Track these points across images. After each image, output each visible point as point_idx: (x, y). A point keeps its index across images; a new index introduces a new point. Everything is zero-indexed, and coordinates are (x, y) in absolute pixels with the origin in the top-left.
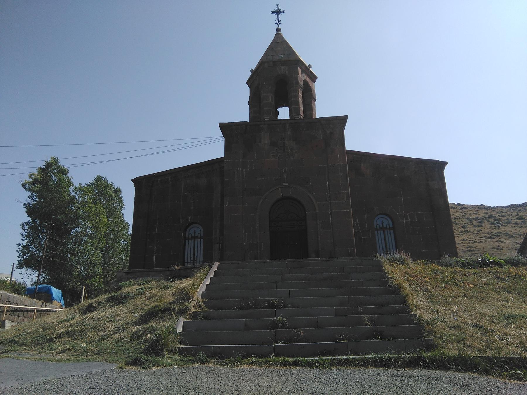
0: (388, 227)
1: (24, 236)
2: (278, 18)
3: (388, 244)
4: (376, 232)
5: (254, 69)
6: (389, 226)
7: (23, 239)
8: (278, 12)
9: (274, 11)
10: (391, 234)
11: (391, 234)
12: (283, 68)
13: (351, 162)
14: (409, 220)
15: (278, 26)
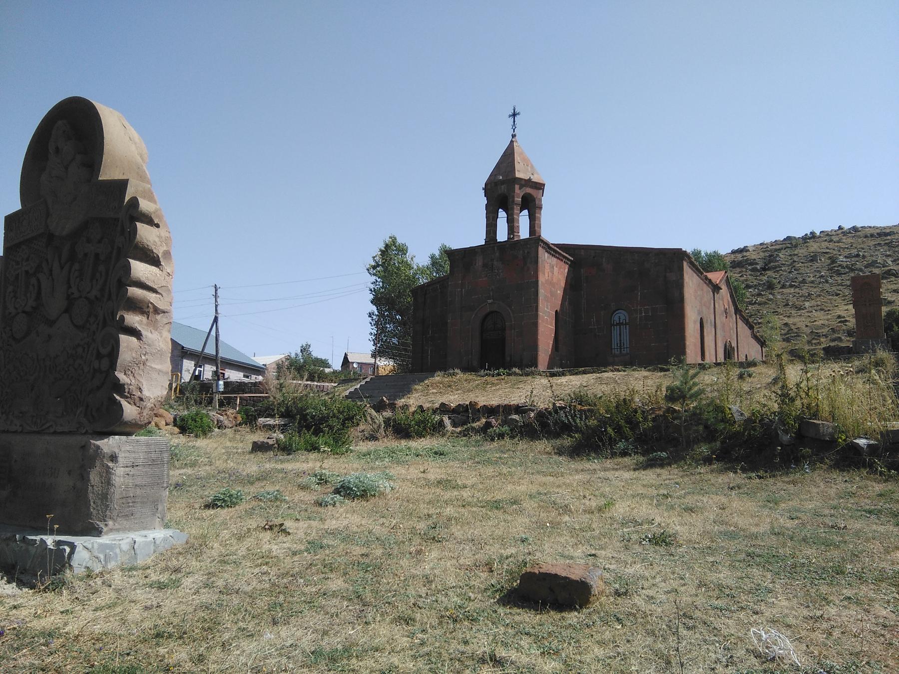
0: (624, 322)
1: (373, 324)
2: (514, 121)
3: (622, 339)
4: (613, 327)
5: (484, 187)
6: (626, 321)
7: (372, 328)
8: (514, 115)
9: (511, 114)
10: (626, 329)
11: (626, 329)
12: (503, 187)
13: (594, 257)
14: (643, 314)
15: (514, 132)
